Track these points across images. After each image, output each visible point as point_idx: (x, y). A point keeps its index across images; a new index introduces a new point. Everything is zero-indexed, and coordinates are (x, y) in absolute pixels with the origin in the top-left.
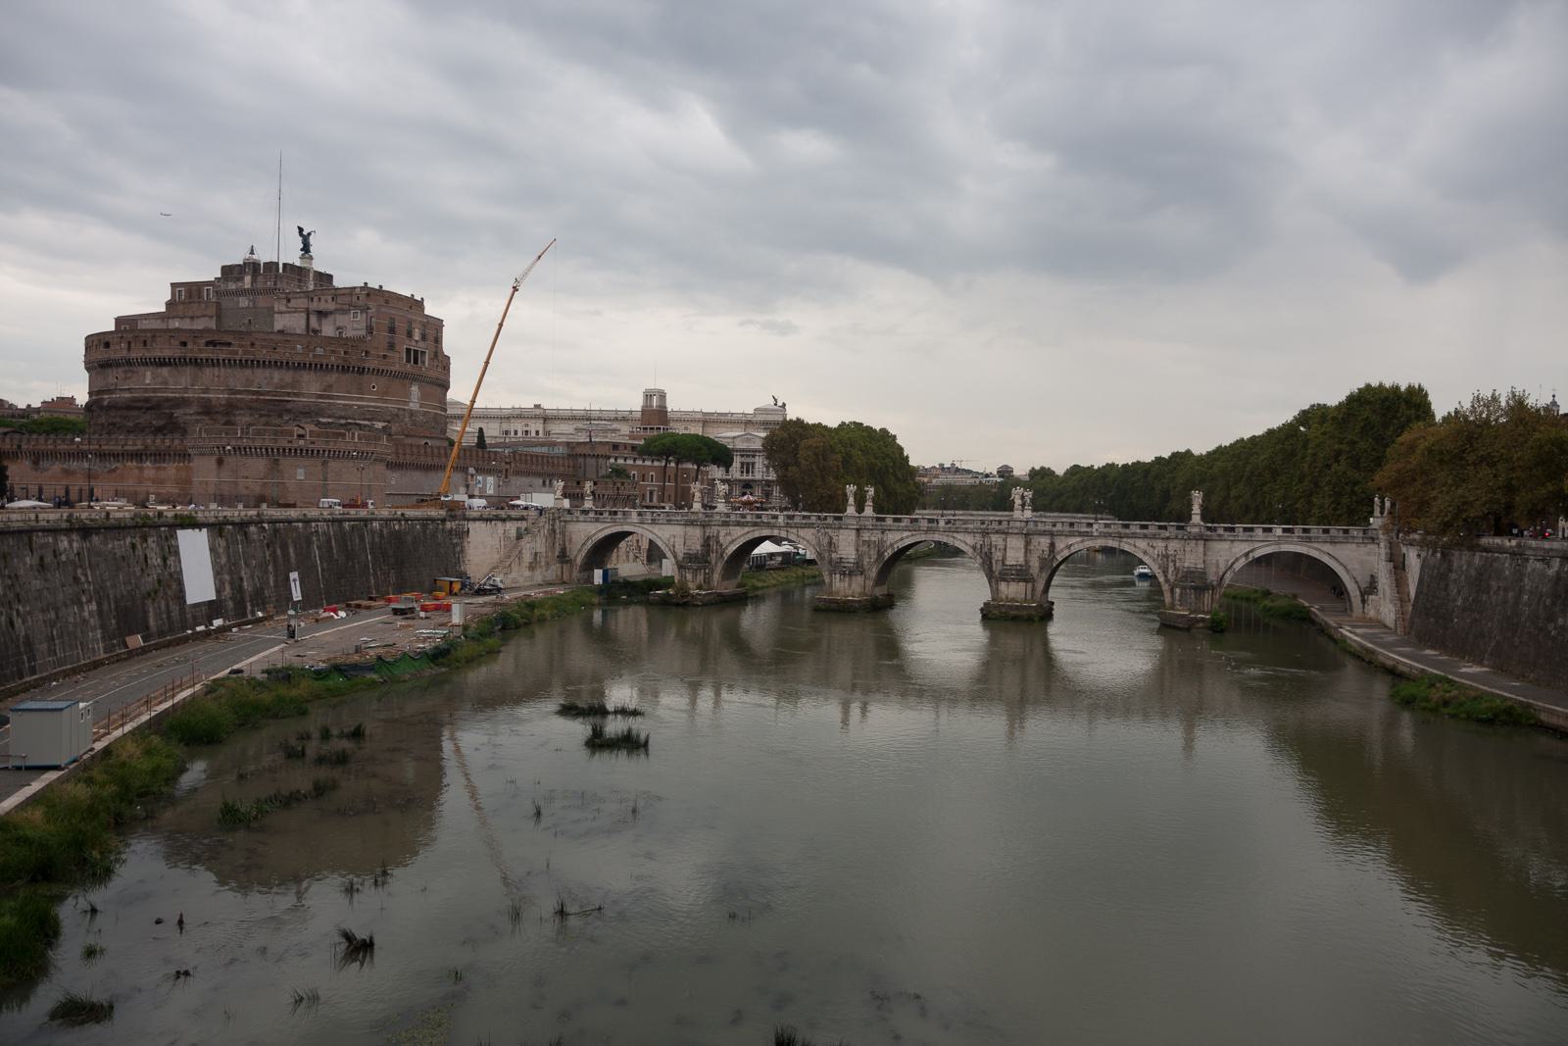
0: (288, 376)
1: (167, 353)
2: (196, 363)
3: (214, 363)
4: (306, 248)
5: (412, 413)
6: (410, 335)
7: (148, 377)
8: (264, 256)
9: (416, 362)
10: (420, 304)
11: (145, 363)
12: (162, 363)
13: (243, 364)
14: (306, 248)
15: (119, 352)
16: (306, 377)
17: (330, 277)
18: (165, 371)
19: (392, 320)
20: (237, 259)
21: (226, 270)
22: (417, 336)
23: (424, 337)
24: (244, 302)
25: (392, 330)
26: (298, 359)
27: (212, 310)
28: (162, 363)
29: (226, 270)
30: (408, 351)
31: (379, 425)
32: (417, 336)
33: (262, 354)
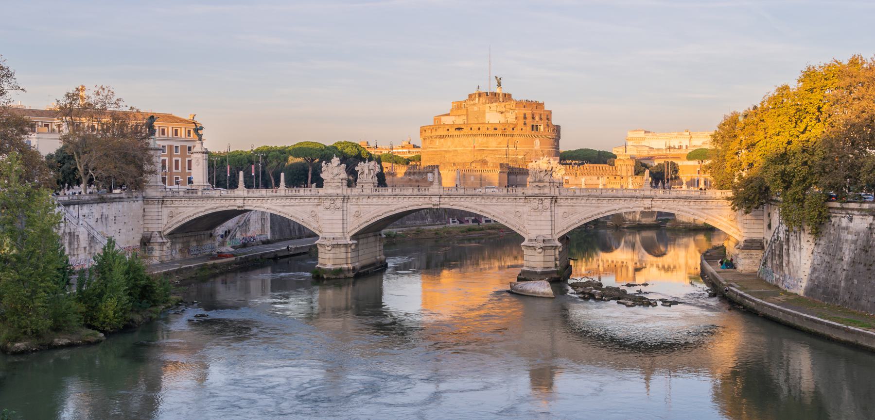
0: (484, 139)
1: (443, 134)
2: (452, 136)
3: (458, 136)
4: (499, 85)
5: (536, 151)
6: (533, 118)
7: (438, 142)
8: (482, 90)
9: (537, 129)
10: (542, 105)
11: (436, 137)
12: (441, 137)
13: (468, 136)
14: (499, 85)
15: (428, 134)
16: (491, 139)
17: (510, 95)
18: (442, 140)
19: (525, 115)
20: (474, 91)
21: (470, 96)
22: (537, 118)
23: (541, 119)
24: (476, 109)
25: (525, 118)
26: (488, 132)
27: (465, 113)
28: (441, 137)
29: (470, 96)
30: (533, 126)
31: (520, 157)
32: (537, 118)
33: (475, 132)
